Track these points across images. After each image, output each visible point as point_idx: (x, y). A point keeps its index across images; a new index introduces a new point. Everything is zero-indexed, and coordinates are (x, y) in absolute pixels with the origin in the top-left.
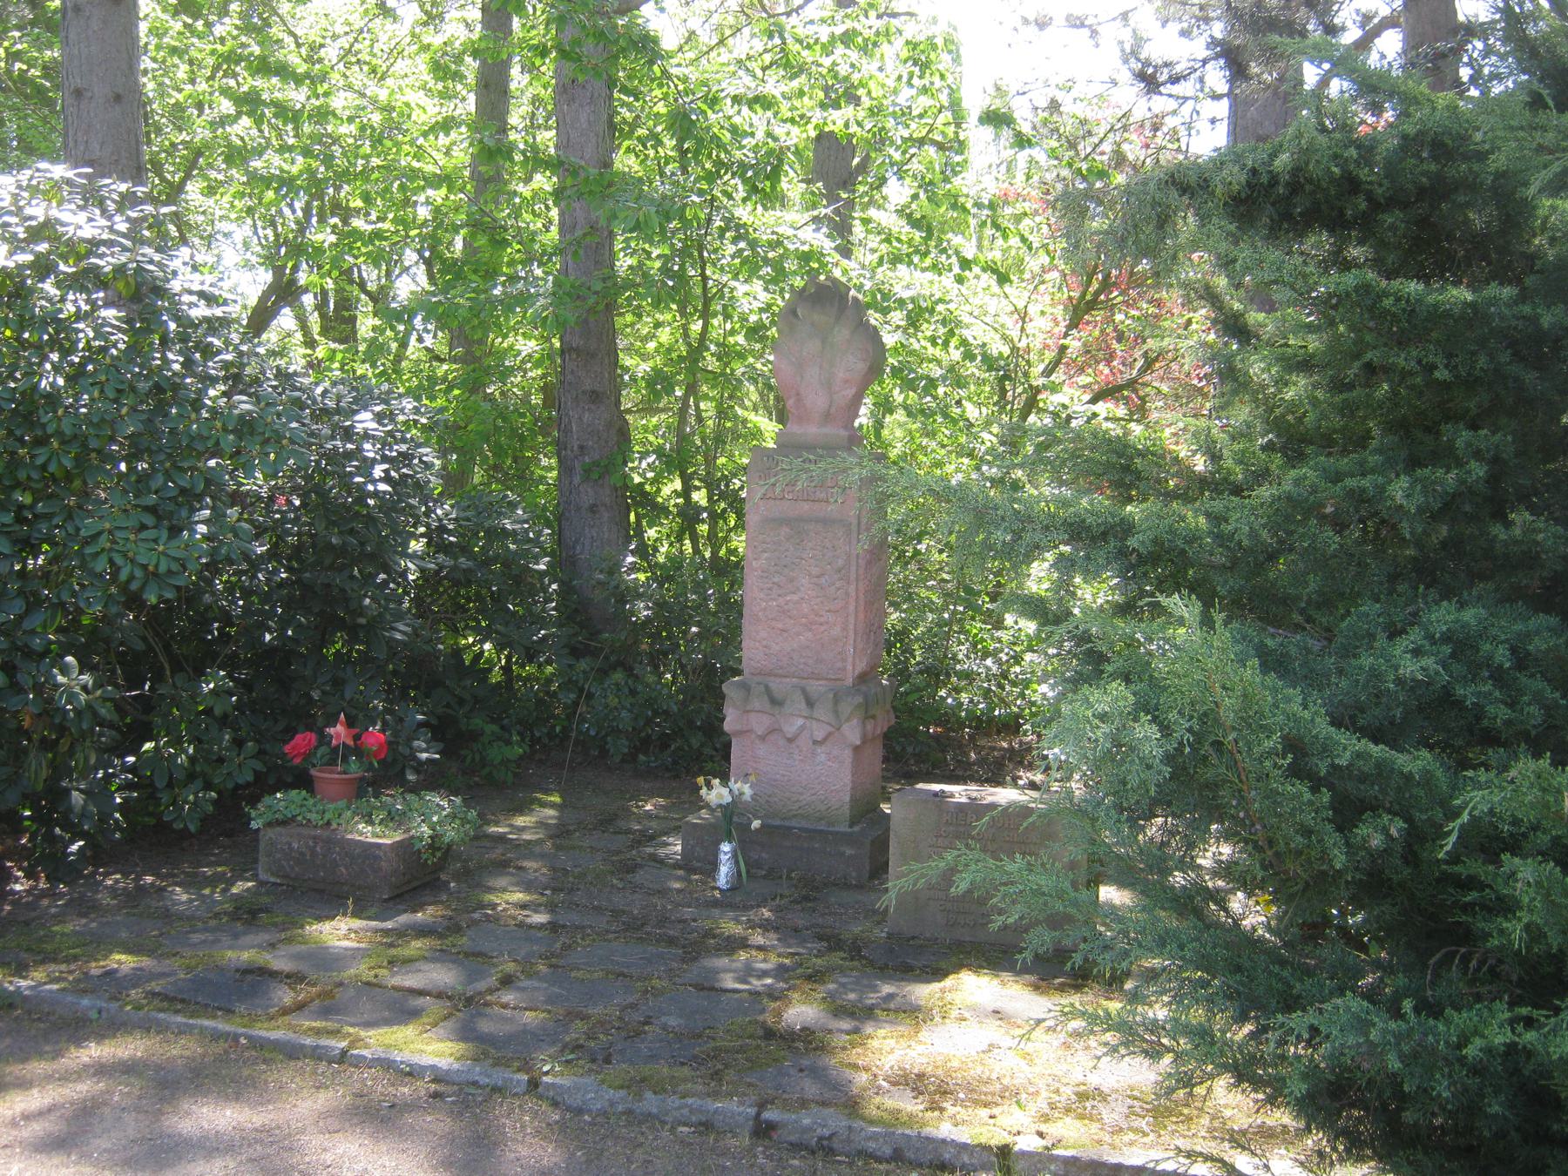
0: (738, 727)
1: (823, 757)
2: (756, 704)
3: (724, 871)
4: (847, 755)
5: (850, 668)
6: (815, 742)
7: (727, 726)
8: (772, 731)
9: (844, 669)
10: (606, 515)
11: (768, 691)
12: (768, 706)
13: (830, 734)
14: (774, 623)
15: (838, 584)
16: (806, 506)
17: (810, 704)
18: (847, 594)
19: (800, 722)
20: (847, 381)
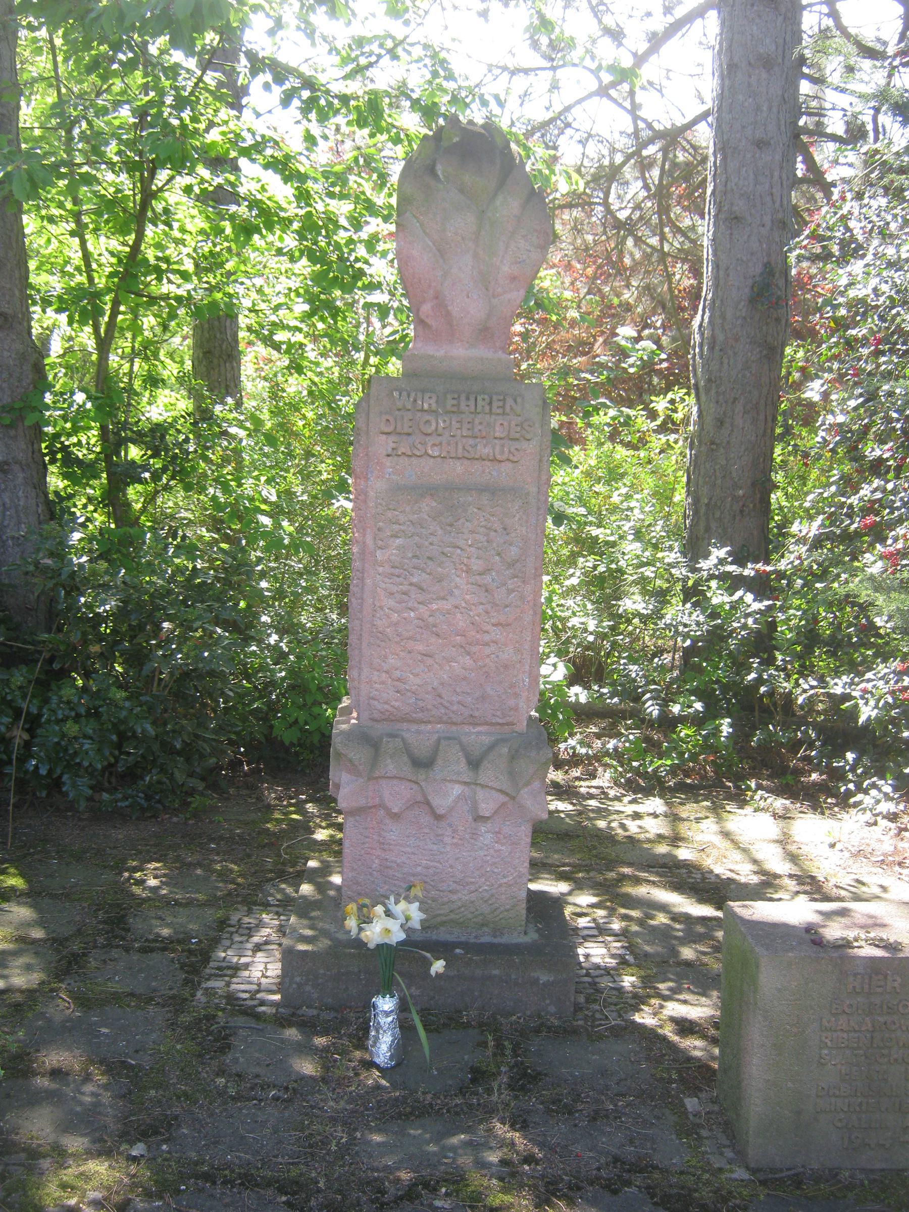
0: (362, 802)
1: (488, 838)
2: (390, 767)
3: (383, 1047)
8: (413, 804)
10: (21, 475)
12: (407, 770)
13: (504, 804)
16: (459, 467)
17: (474, 764)
18: (522, 598)
20: (513, 279)
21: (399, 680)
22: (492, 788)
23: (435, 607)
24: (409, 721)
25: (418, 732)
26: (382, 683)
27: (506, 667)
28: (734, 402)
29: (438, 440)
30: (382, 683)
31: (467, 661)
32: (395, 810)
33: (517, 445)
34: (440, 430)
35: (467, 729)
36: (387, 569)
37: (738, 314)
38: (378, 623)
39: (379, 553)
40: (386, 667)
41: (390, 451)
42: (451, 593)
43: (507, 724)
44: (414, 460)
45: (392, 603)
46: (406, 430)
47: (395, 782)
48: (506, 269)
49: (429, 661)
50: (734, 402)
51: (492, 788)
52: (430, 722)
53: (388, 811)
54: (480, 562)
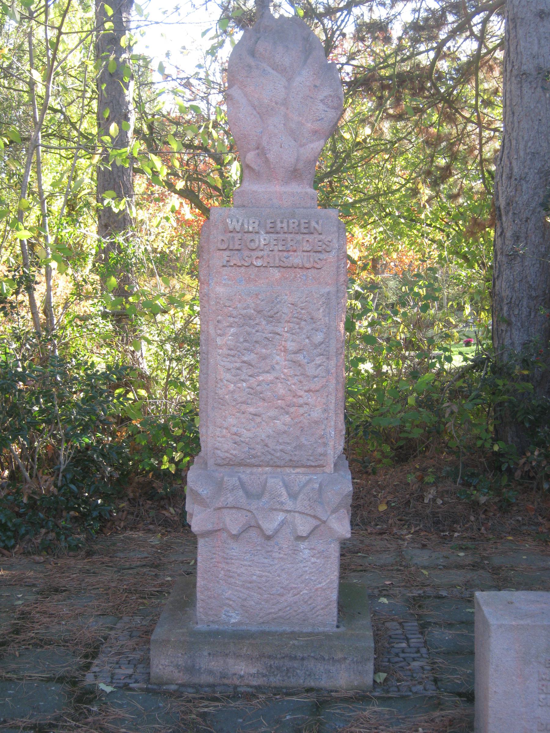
0: (210, 527)
4: (334, 551)
5: (330, 452)
6: (300, 538)
7: (195, 528)
8: (247, 528)
9: (325, 455)
11: (242, 485)
13: (316, 527)
14: (244, 407)
15: (318, 360)
18: (328, 371)
19: (280, 516)
20: (315, 132)
21: (235, 434)
22: (307, 515)
23: (261, 378)
24: (245, 465)
25: (252, 474)
26: (224, 437)
27: (316, 422)
28: (526, 221)
29: (260, 254)
30: (224, 437)
31: (287, 419)
32: (234, 532)
33: (321, 256)
34: (262, 246)
35: (288, 470)
36: (225, 351)
37: (528, 151)
38: (220, 392)
39: (218, 339)
40: (225, 425)
41: (225, 263)
42: (273, 368)
43: (319, 466)
44: (243, 269)
45: (228, 376)
46: (237, 247)
47: (234, 511)
48: (309, 125)
49: (258, 420)
50: (526, 221)
51: (307, 515)
52: (260, 466)
53: (228, 532)
54: (293, 344)
